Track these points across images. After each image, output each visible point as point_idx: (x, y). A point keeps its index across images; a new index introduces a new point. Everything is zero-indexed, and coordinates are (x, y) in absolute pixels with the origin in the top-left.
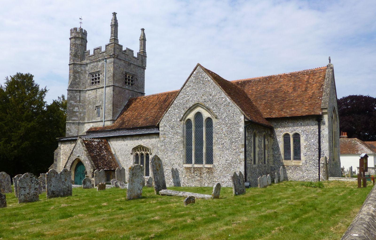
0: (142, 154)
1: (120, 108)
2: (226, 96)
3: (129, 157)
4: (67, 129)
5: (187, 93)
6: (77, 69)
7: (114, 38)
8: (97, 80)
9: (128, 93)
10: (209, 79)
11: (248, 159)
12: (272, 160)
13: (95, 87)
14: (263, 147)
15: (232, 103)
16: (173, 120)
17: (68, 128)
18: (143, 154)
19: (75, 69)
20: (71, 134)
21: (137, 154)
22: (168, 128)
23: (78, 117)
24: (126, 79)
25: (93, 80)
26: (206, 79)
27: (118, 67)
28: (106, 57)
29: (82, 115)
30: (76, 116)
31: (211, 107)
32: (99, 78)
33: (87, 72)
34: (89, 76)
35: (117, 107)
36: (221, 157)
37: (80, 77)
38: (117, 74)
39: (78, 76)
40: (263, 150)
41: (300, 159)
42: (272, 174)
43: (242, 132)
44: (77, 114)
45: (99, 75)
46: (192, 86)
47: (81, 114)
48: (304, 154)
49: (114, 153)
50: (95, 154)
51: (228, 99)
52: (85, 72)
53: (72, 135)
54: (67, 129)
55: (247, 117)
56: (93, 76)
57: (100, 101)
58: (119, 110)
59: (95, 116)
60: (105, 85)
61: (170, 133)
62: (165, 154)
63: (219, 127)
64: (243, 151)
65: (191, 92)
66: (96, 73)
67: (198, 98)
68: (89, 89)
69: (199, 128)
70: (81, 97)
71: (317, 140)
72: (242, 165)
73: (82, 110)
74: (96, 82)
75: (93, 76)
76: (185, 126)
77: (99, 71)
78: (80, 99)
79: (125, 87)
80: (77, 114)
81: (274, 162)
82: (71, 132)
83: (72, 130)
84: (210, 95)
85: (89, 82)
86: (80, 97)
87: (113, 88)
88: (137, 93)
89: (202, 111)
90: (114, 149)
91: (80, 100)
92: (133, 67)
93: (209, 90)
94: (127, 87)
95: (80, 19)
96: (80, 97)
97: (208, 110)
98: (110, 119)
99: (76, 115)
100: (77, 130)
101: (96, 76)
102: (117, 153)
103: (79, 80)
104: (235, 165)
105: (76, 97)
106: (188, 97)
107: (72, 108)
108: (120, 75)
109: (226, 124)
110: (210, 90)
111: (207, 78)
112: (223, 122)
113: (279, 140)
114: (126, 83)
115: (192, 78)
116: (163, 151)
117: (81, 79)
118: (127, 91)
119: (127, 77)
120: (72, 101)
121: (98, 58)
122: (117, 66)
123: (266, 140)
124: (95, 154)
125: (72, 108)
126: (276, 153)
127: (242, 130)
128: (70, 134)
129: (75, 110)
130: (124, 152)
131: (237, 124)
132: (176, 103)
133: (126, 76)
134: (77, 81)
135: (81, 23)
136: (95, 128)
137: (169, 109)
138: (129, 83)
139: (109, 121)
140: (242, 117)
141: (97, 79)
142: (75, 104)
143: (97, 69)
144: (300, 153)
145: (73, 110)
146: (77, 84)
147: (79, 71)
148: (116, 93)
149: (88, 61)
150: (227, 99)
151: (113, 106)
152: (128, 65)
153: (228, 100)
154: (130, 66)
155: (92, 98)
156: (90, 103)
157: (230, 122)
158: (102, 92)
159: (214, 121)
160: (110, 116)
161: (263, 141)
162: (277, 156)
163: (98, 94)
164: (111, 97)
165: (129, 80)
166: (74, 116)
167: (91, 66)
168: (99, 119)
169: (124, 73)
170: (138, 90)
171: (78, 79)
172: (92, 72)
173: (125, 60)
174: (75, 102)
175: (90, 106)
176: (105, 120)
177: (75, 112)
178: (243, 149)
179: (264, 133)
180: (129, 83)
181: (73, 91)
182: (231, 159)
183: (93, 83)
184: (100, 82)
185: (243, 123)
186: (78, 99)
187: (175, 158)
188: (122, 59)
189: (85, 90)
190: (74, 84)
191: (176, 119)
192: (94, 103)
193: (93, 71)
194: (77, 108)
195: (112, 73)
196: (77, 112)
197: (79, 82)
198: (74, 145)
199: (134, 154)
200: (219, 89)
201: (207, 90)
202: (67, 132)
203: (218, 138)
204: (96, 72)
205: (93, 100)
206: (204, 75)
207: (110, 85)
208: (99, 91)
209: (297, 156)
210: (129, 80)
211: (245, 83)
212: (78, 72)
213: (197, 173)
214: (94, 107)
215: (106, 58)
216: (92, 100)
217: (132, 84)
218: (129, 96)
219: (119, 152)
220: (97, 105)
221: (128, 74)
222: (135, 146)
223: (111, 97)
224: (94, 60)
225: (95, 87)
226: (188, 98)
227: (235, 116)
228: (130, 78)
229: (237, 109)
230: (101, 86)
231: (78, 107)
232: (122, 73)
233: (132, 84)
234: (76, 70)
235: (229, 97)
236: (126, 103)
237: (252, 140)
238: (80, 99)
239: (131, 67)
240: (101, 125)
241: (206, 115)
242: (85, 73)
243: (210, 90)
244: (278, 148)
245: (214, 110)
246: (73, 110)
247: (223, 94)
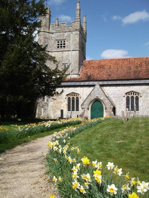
0: (132, 97)
3: (121, 99)
8: (63, 45)
13: (61, 50)
21: (128, 97)
32: (64, 44)
33: (53, 39)
34: (55, 41)
45: (64, 42)
52: (52, 39)
56: (58, 42)
68: (55, 51)
75: (58, 42)
90: (107, 93)
98: (76, 73)
101: (61, 42)
121: (64, 30)
176: (72, 74)
183: (58, 47)
193: (59, 38)
198: (93, 88)
199: (126, 96)
207: (77, 49)
212: (47, 38)
216: (58, 59)
219: (113, 95)
222: (127, 91)
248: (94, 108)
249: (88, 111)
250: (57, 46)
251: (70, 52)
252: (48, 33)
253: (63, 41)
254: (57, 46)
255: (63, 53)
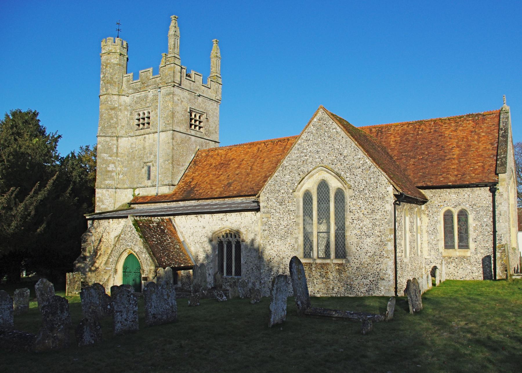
1: (183, 166)
2: (365, 156)
4: (98, 199)
5: (305, 151)
6: (113, 104)
7: (173, 55)
9: (195, 141)
10: (339, 130)
11: (398, 250)
12: (427, 249)
14: (415, 230)
15: (375, 168)
16: (283, 191)
17: (99, 198)
18: (231, 242)
19: (109, 103)
20: (102, 207)
22: (273, 203)
23: (114, 180)
24: (191, 119)
25: (139, 120)
26: (334, 130)
27: (180, 102)
28: (160, 85)
29: (121, 176)
30: (112, 178)
31: (342, 173)
32: (149, 118)
34: (131, 114)
35: (179, 165)
36: (358, 249)
37: (117, 116)
38: (178, 112)
39: (114, 115)
40: (416, 235)
41: (467, 247)
42: (427, 270)
43: (389, 211)
44: (114, 174)
45: (149, 113)
46: (311, 139)
47: (119, 174)
48: (473, 240)
49: (182, 239)
50: (155, 241)
51: (369, 162)
53: (105, 209)
54: (98, 199)
55: (398, 188)
56: (139, 115)
57: (151, 154)
58: (181, 169)
59: (143, 178)
60: (159, 130)
61: (278, 210)
62: (270, 242)
63: (355, 202)
64: (392, 239)
65: (311, 149)
66: (144, 110)
67: (322, 159)
69: (322, 204)
70: (119, 148)
71: (492, 220)
72: (390, 260)
73: (120, 168)
74: (144, 124)
76: (301, 200)
77: (148, 107)
78: (117, 150)
79: (191, 132)
80: (114, 174)
81: (430, 251)
82: (103, 204)
83: (105, 201)
84: (341, 154)
85: (131, 124)
86: (117, 148)
87: (173, 134)
88: (208, 141)
89: (328, 179)
91: (117, 153)
92: (202, 100)
93: (338, 147)
94: (193, 133)
95: (117, 24)
96: (117, 148)
97: (338, 175)
99: (111, 176)
100: (113, 201)
101: (144, 114)
102: (187, 240)
103: (116, 120)
104: (379, 259)
105: (111, 148)
106: (306, 156)
107: (104, 166)
108: (183, 113)
109: (366, 199)
110: (341, 147)
111: (336, 128)
112: (361, 196)
113: (437, 218)
114: (191, 125)
115: (312, 127)
116: (266, 239)
117: (120, 118)
118: (193, 138)
119: (193, 116)
120: (105, 155)
122: (178, 100)
123: (418, 219)
124: (155, 241)
125: (104, 166)
126: (432, 238)
127: (389, 207)
128: (101, 207)
129: (110, 169)
130: (199, 238)
131: (382, 198)
132: (286, 164)
133: (191, 115)
134: (112, 122)
135: (119, 30)
136: (143, 197)
137: (276, 174)
138: (195, 126)
139: (166, 185)
140: (390, 189)
141: (146, 119)
142: (110, 158)
143: (146, 104)
144: (467, 238)
145: (106, 168)
146: (113, 128)
147: (116, 106)
148: (176, 142)
149: (131, 91)
150: (367, 161)
151: (172, 163)
152: (195, 98)
153: (368, 163)
154: (198, 99)
155: (136, 149)
156: (134, 158)
157: (371, 196)
158: (154, 141)
159: (348, 193)
160: (167, 179)
161: (415, 220)
162: (434, 242)
163: (147, 144)
164: (168, 149)
165: (196, 121)
166: (109, 177)
167: (135, 98)
168: (149, 183)
169: (189, 110)
170: (208, 137)
171: (114, 119)
172: (137, 108)
173: (189, 90)
174: (109, 156)
175: (134, 162)
177: (109, 171)
178: (393, 236)
179: (416, 209)
180: (195, 126)
181: (107, 138)
182: (374, 250)
184: (150, 124)
185: (391, 197)
186: (115, 150)
187: (285, 249)
188: (185, 88)
189: (126, 136)
190: (107, 126)
191: (286, 190)
192: (141, 158)
194: (113, 166)
195: (170, 111)
196: (112, 171)
197: (117, 123)
200: (353, 145)
201: (336, 146)
202: (97, 204)
203: (353, 220)
204: (144, 108)
205: (138, 152)
206: (331, 123)
207: (168, 128)
208: (149, 139)
209: (464, 244)
210: (196, 121)
211: (381, 130)
212: (113, 109)
213: (322, 272)
214: (140, 164)
215: (160, 86)
216: (137, 153)
217: (200, 128)
218: (196, 147)
220: (146, 161)
221: (195, 112)
223: (168, 149)
224: (140, 89)
225: (143, 131)
226: (306, 158)
227: (379, 187)
228: (197, 118)
229: (384, 178)
230: (153, 131)
231: (114, 163)
232: (186, 110)
233: (200, 128)
234: (112, 104)
235: (370, 158)
236: (192, 157)
237: (403, 221)
238: (117, 150)
239: (198, 101)
240: (152, 192)
241: (334, 184)
242: (125, 110)
243: (341, 147)
244: (435, 231)
245: (347, 178)
246: (106, 168)
247: (361, 154)
248: (128, 270)
249: (115, 276)
250: (137, 122)
251: (156, 134)
252: (116, 97)
253: (146, 112)
254: (137, 122)
255: (145, 138)
